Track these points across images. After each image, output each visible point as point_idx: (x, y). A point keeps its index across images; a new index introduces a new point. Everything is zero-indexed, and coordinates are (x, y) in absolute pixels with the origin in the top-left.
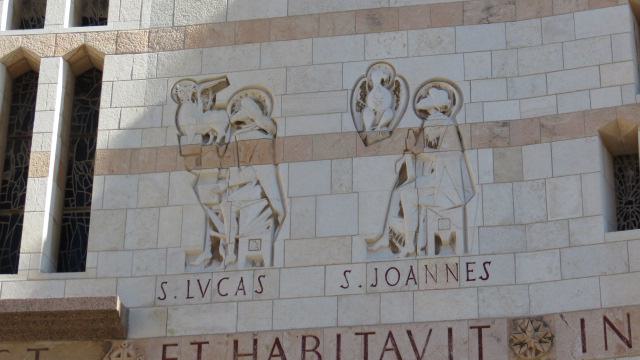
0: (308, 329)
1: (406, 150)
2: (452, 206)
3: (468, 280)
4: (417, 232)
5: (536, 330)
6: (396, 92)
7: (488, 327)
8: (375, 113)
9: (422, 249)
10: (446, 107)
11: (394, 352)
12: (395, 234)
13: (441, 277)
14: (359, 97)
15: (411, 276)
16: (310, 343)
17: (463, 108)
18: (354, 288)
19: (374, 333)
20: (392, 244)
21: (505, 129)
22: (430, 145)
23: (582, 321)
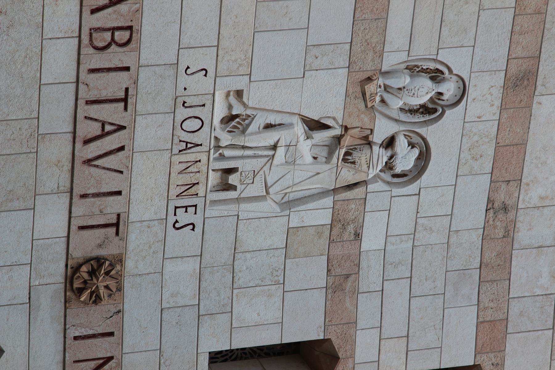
0: (140, 32)
1: (346, 129)
2: (269, 185)
3: (176, 208)
4: (244, 147)
5: (107, 287)
6: (425, 110)
7: (117, 234)
8: (400, 89)
9: (220, 154)
10: (391, 168)
11: (99, 132)
12: (244, 120)
13: (187, 179)
14: (424, 68)
15: (189, 146)
16: (121, 35)
17: (387, 188)
18: (183, 80)
19: (126, 108)
20: (232, 118)
21: (352, 237)
22: (347, 154)
23: (111, 334)
